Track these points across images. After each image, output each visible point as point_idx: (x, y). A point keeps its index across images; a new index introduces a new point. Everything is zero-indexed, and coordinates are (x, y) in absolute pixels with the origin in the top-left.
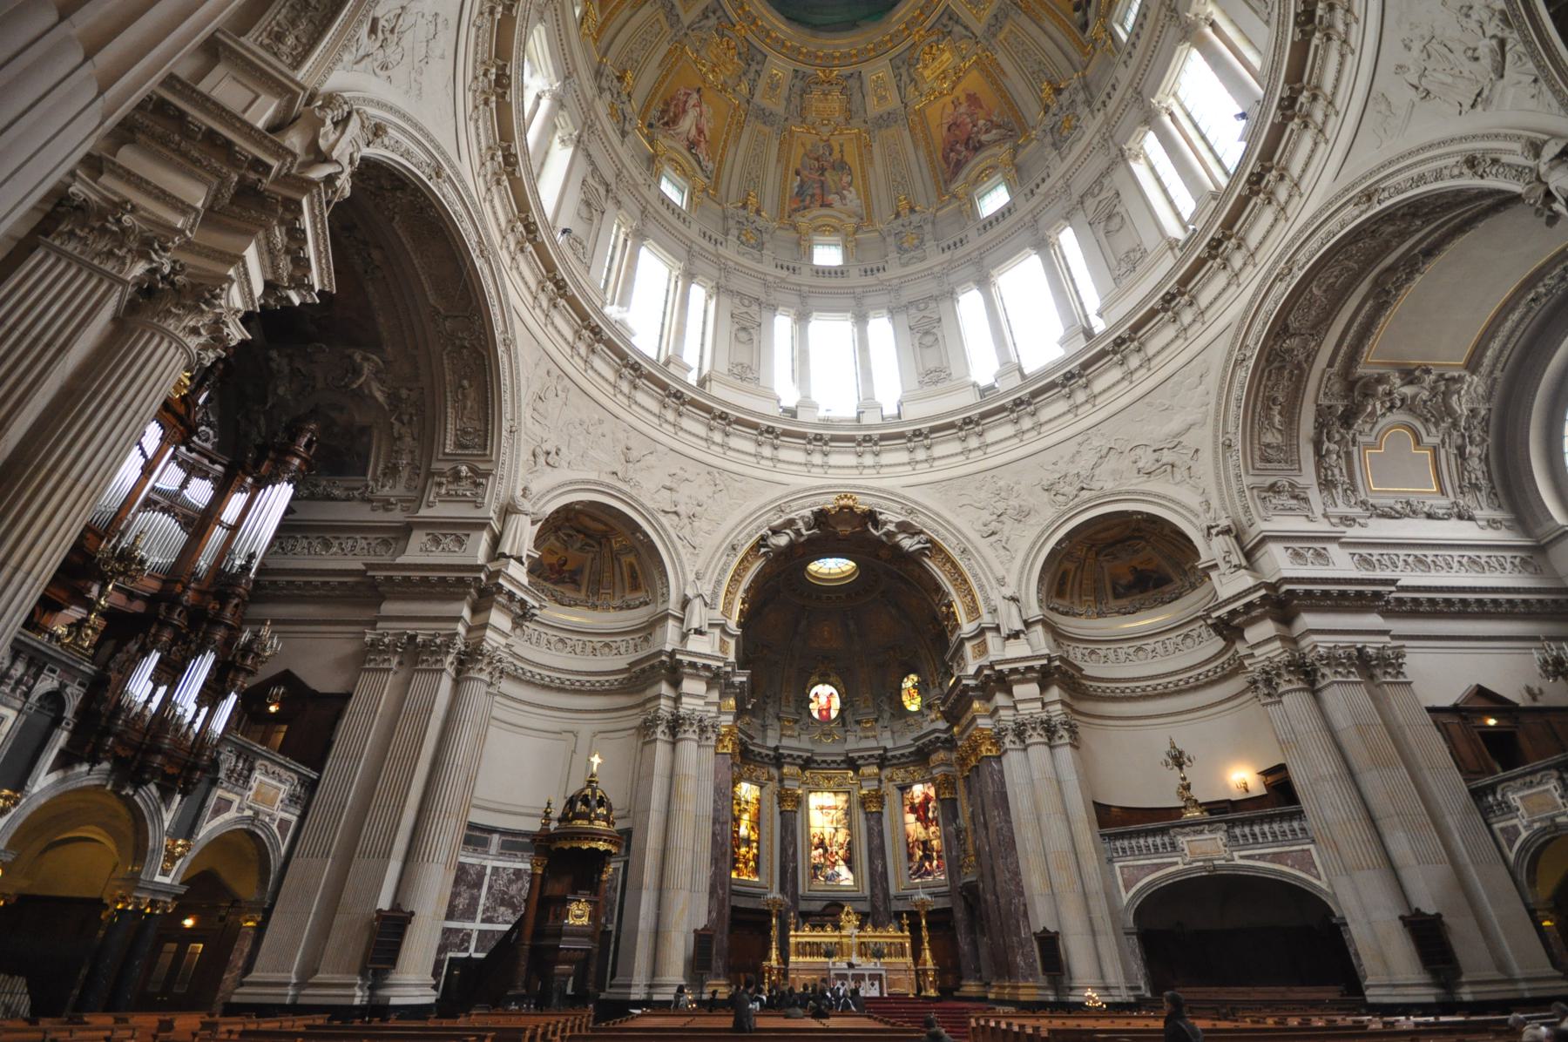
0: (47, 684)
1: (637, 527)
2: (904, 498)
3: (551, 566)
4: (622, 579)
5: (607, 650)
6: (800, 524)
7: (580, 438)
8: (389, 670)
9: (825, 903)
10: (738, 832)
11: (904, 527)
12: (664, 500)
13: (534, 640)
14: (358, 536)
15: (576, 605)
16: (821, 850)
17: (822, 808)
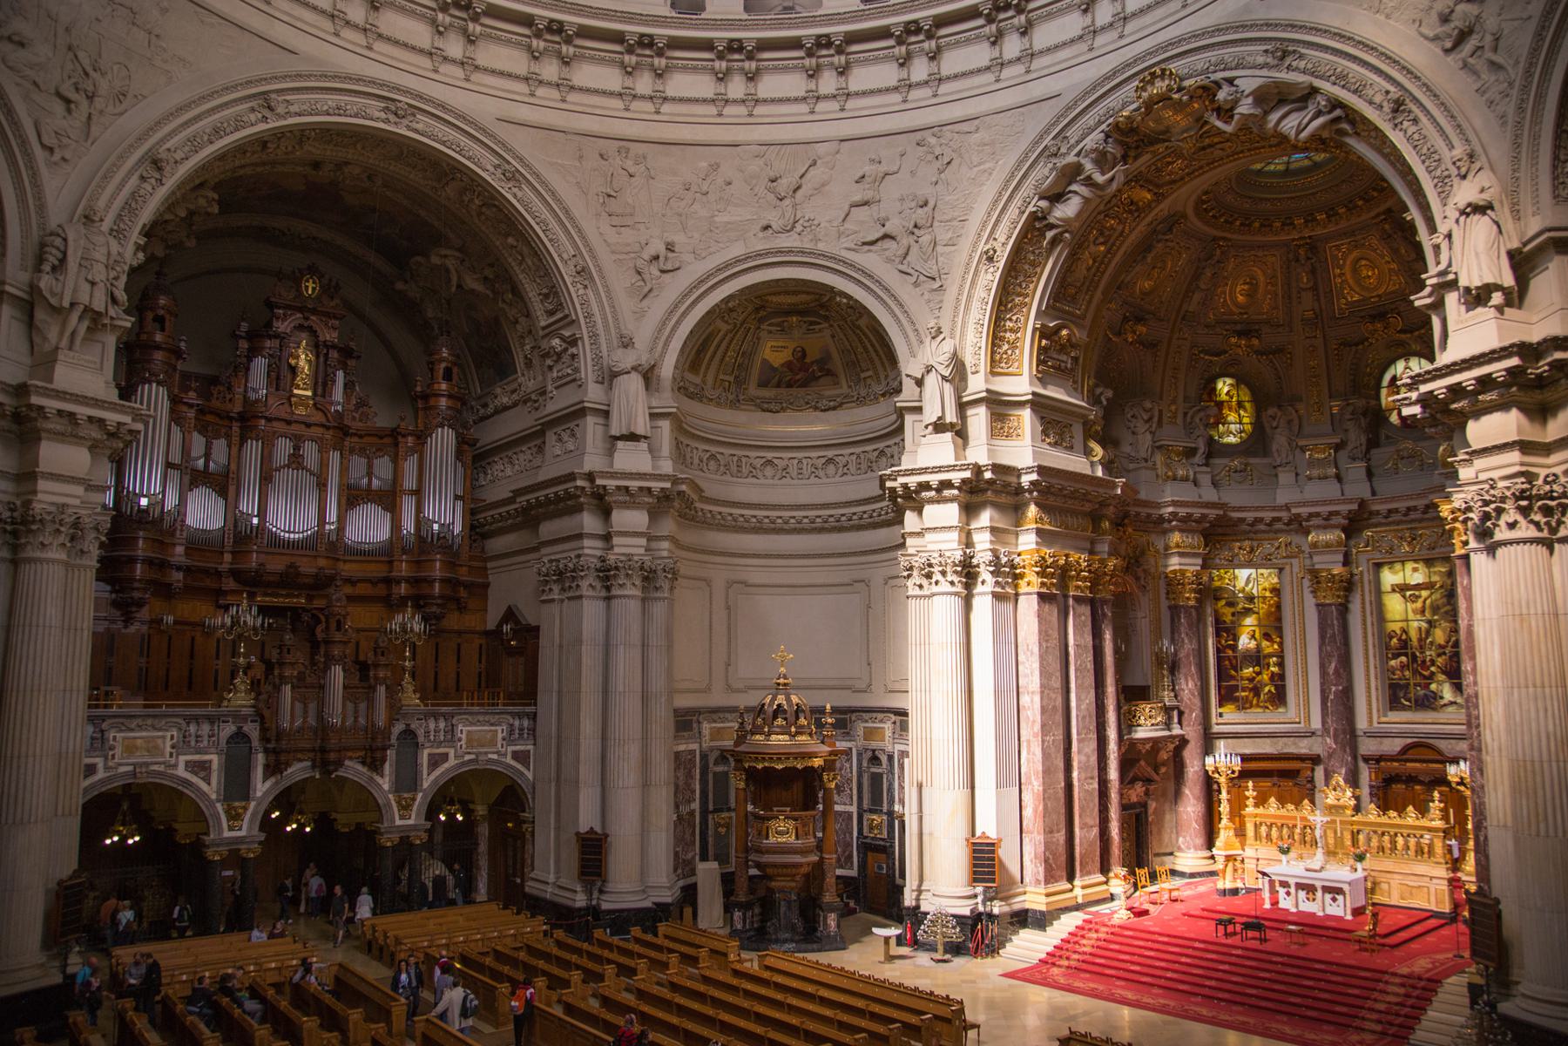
0: (229, 729)
1: (831, 289)
2: (1268, 25)
3: (788, 365)
4: (876, 351)
5: (884, 459)
6: (1088, 166)
7: (696, 206)
8: (553, 600)
9: (1410, 741)
10: (1234, 648)
11: (1274, 97)
12: (864, 224)
13: (794, 474)
14: (510, 454)
15: (841, 405)
16: (1404, 659)
17: (1402, 589)
